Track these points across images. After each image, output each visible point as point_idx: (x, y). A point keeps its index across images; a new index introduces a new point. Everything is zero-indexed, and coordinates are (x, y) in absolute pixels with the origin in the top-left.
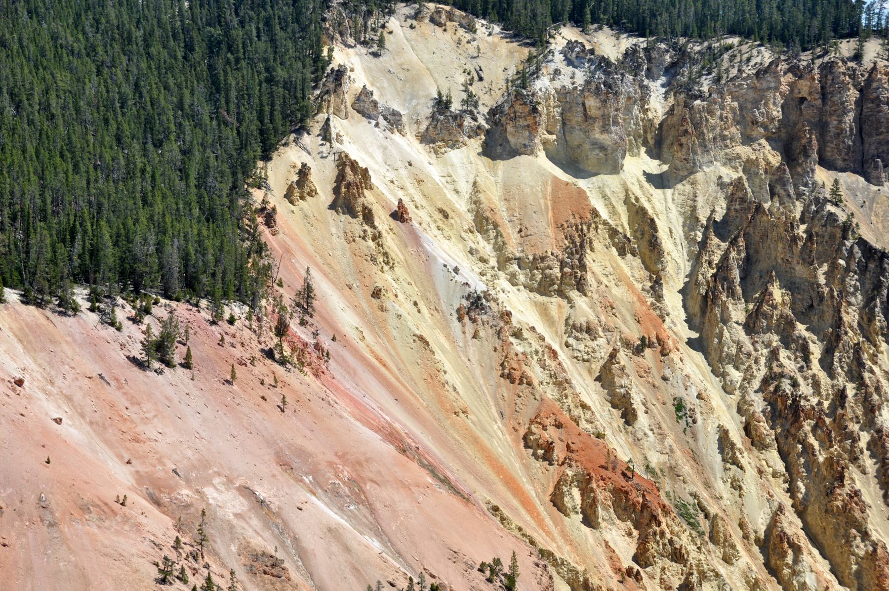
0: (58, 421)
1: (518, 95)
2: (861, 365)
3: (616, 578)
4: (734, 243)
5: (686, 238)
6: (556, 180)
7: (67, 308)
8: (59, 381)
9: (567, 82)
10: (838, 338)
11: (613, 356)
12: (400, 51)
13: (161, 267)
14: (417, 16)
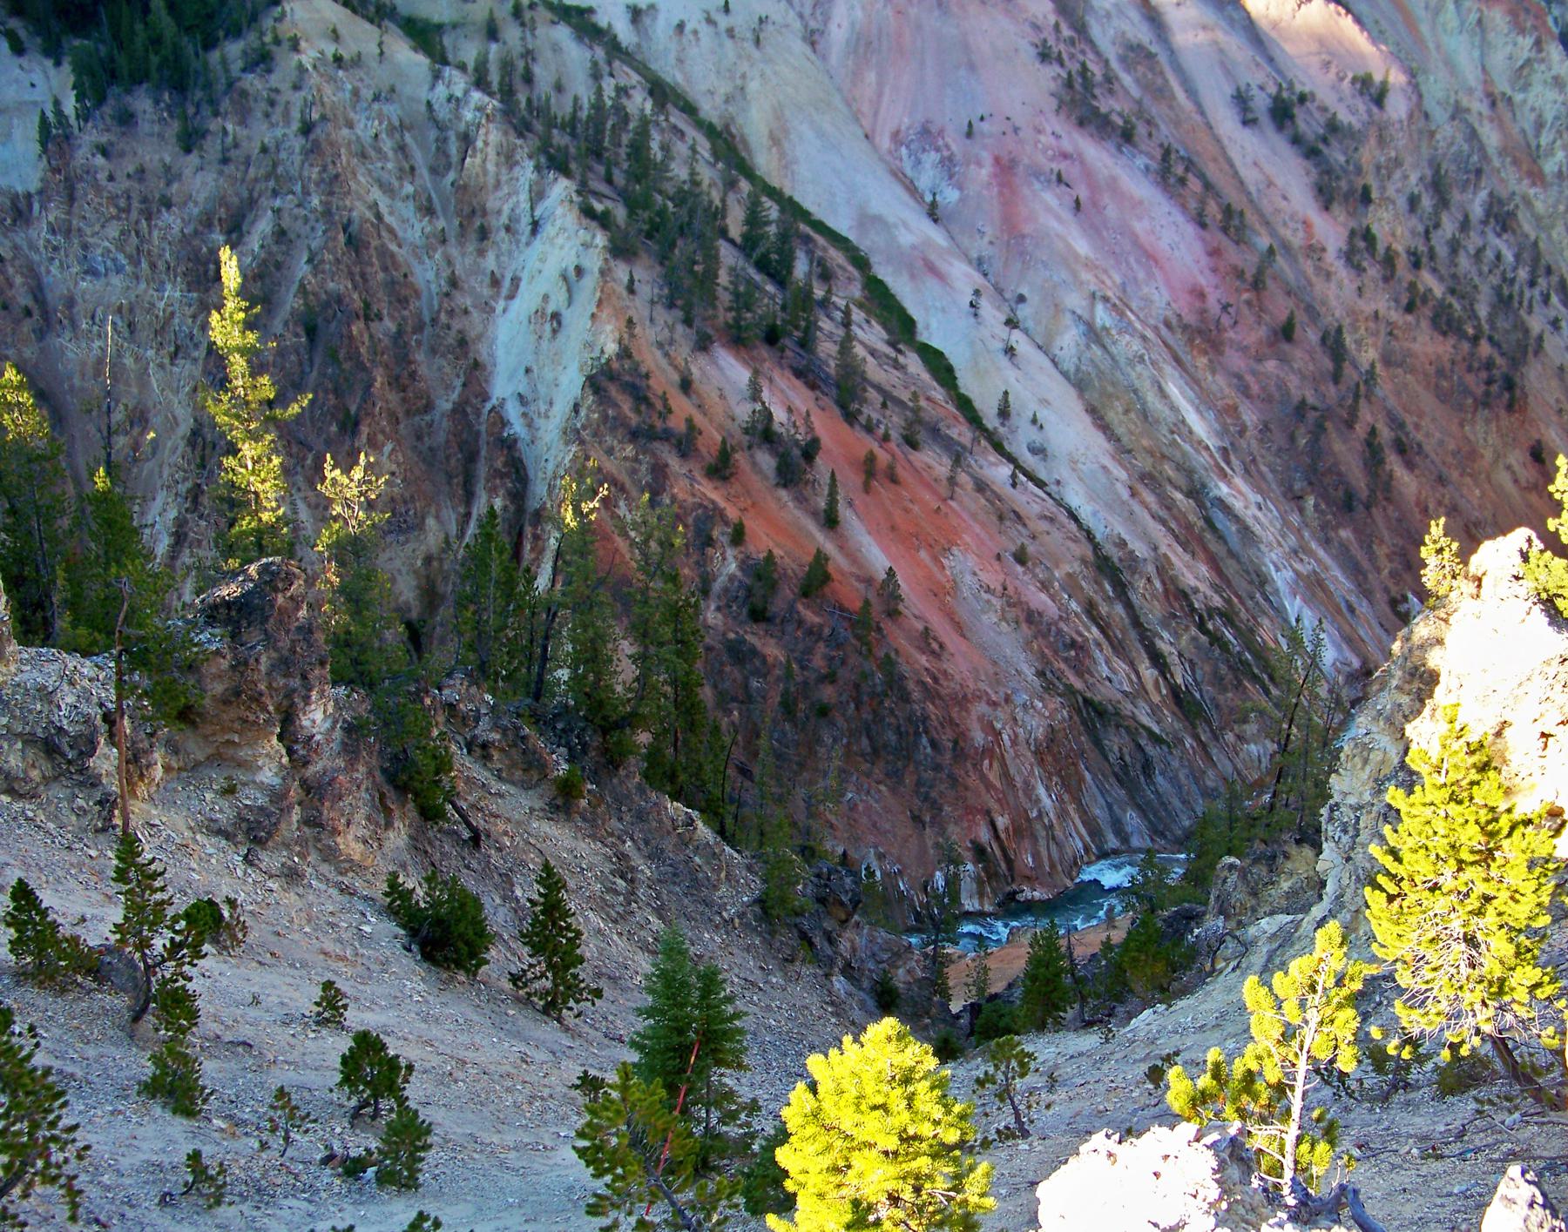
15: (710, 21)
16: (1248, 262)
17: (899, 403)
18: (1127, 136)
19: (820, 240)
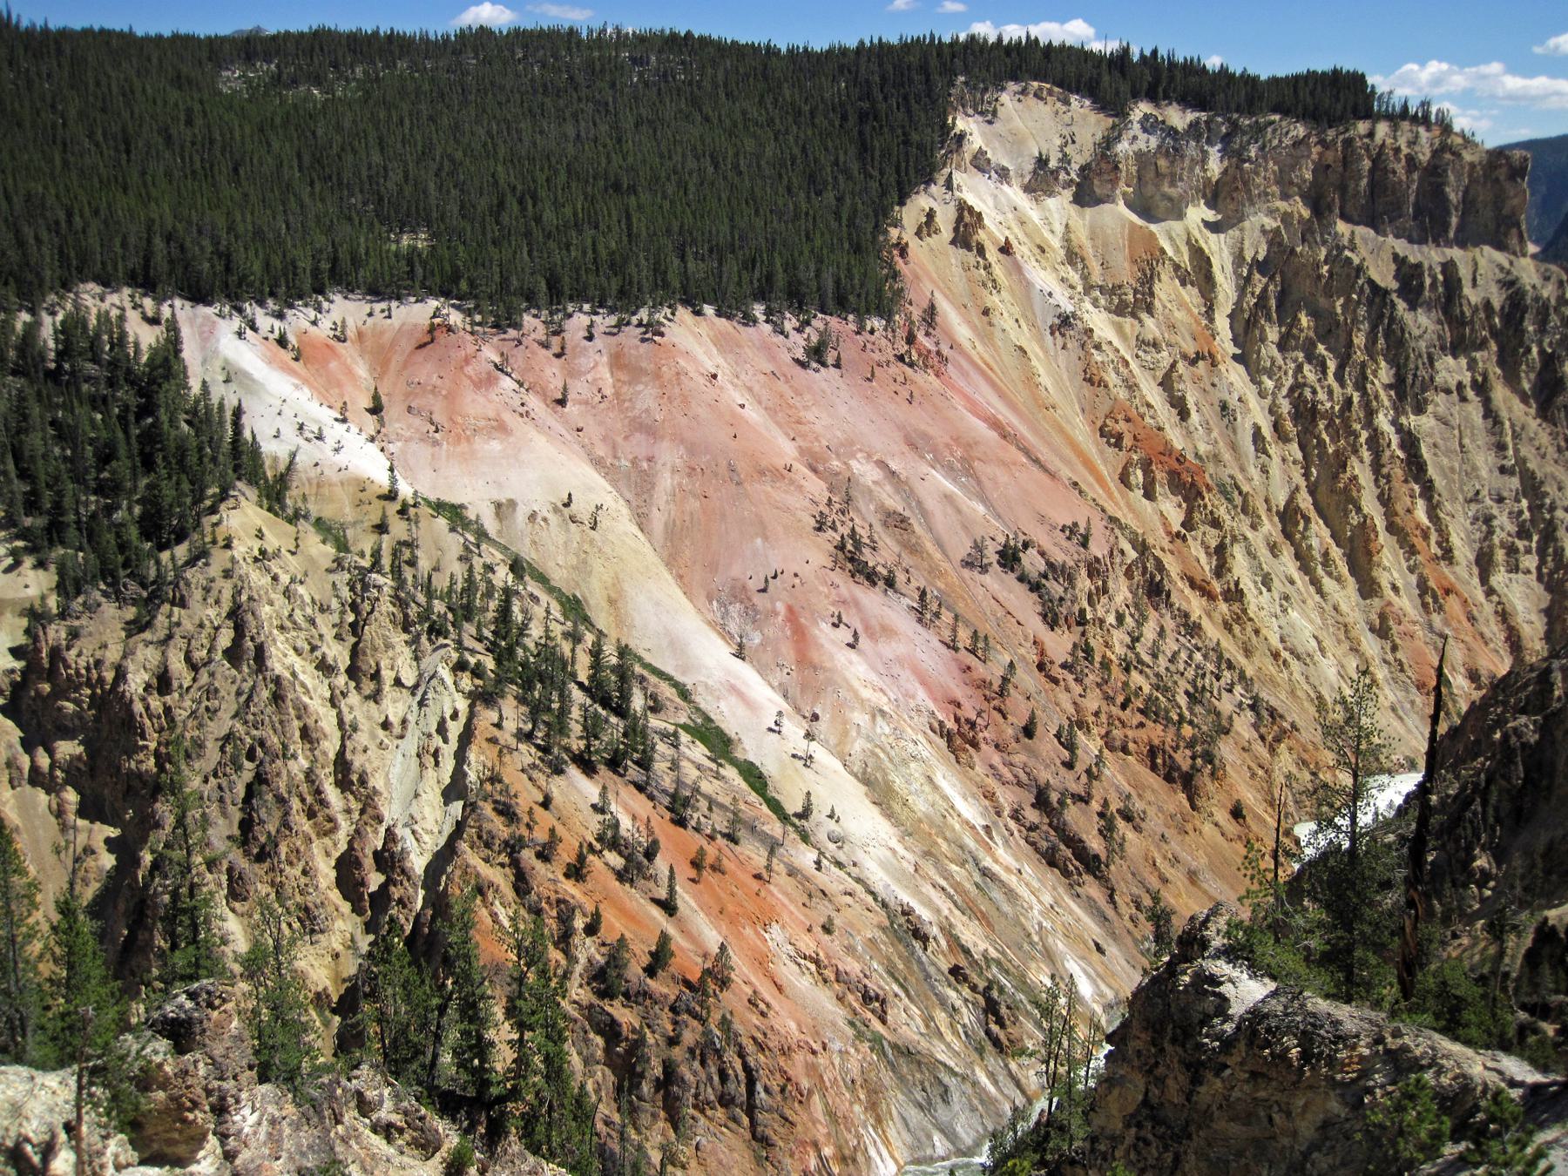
0: (742, 406)
1: (1104, 156)
2: (1366, 378)
3: (1168, 539)
4: (1272, 278)
5: (1235, 272)
6: (1132, 224)
7: (749, 320)
8: (743, 376)
9: (1143, 147)
10: (1349, 356)
11: (1173, 365)
12: (1010, 120)
13: (819, 289)
14: (1024, 92)
15: (556, 510)
16: (993, 672)
17: (722, 806)
18: (890, 583)
19: (653, 679)
